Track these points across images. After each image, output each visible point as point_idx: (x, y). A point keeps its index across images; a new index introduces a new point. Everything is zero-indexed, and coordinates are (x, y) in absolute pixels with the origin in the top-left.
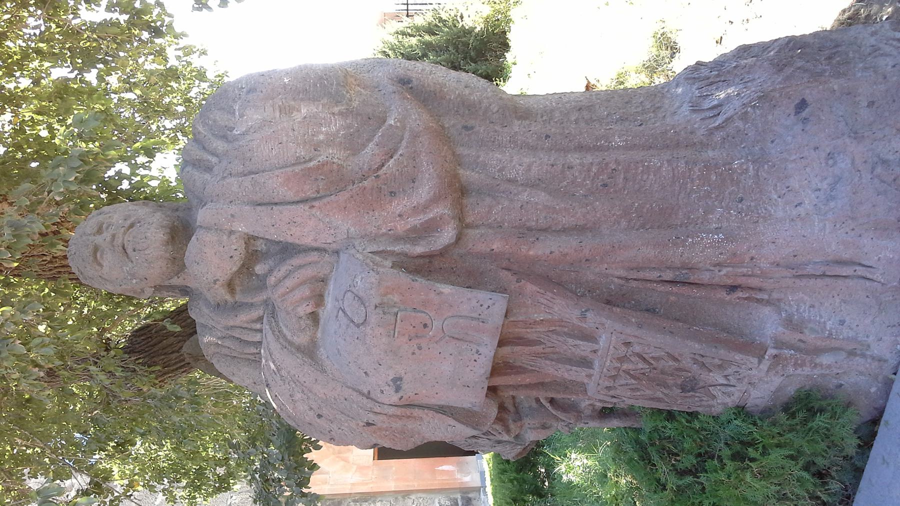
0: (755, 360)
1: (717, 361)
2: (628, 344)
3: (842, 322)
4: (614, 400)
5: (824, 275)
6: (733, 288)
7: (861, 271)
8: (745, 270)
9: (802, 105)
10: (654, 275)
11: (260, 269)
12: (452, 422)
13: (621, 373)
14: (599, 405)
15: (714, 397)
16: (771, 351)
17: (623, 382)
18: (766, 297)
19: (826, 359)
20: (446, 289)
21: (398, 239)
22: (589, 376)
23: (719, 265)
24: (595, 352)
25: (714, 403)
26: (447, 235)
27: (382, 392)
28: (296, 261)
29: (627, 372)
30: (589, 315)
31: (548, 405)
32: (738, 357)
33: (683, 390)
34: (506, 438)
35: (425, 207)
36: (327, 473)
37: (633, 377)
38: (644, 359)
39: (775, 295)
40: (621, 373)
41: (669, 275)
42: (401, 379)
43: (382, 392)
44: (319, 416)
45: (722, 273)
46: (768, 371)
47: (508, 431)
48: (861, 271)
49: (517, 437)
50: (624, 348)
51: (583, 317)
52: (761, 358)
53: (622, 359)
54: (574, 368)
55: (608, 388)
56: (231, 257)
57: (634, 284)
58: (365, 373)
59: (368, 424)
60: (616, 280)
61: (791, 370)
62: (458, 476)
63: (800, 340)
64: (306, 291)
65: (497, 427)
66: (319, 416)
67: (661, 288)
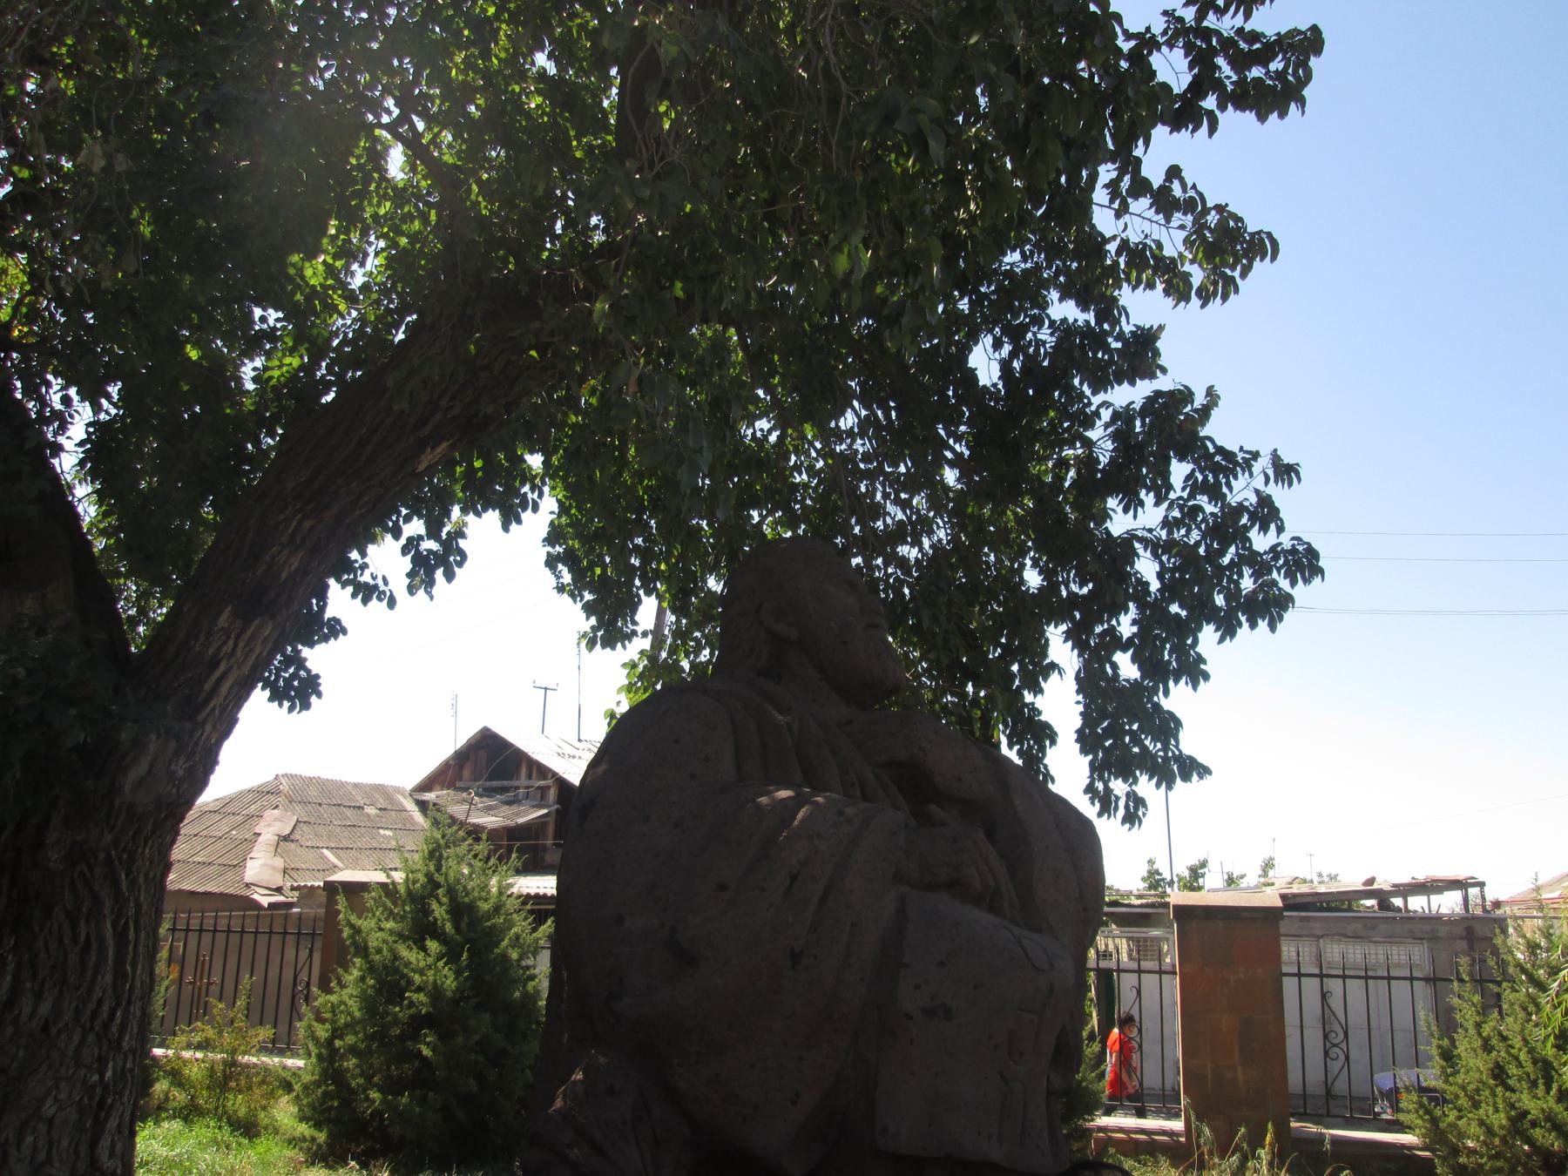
27: (917, 987)
43: (917, 987)
44: (794, 878)
56: (960, 779)
58: (941, 964)
59: (796, 958)
66: (794, 878)
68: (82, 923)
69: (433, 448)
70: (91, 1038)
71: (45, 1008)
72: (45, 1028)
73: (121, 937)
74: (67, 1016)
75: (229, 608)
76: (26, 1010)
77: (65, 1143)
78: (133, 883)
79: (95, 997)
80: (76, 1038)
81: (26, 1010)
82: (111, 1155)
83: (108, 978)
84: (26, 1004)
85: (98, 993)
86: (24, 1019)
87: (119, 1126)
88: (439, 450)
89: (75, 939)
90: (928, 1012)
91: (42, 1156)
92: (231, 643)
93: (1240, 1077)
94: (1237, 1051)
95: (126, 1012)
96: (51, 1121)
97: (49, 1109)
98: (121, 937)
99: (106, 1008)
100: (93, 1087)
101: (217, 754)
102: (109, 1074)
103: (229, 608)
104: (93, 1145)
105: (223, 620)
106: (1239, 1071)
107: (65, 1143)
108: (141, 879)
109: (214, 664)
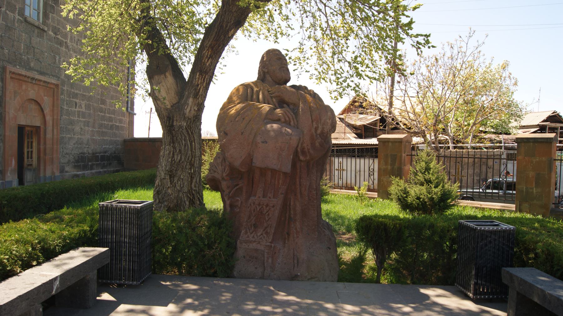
0: (270, 240)
1: (269, 231)
2: (273, 206)
3: (279, 264)
4: (249, 205)
5: (294, 256)
6: (288, 234)
7: (296, 265)
8: (295, 235)
9: (330, 249)
10: (292, 212)
11: (285, 105)
12: (243, 158)
13: (261, 206)
14: (239, 203)
15: (252, 233)
16: (273, 245)
17: (258, 207)
18: (287, 242)
19: (270, 260)
20: (292, 157)
21: (302, 144)
22: (259, 197)
23: (296, 229)
24: (270, 198)
25: (249, 234)
26: (302, 158)
28: (294, 116)
29: (262, 207)
30: (283, 195)
31: (237, 187)
32: (271, 237)
33: (254, 224)
34: (224, 175)
35: (309, 152)
36: (14, 100)
37: (260, 209)
38: (267, 212)
39: (286, 245)
40: (261, 206)
41: (292, 216)
42: (267, 143)
44: (244, 119)
45: (295, 230)
46: (266, 245)
47: (226, 176)
48: (296, 265)
49: (223, 179)
50: (272, 205)
51: (282, 194)
52: (271, 243)
53: (267, 206)
54: (262, 192)
55: (254, 203)
57: (288, 207)
60: (289, 203)
61: (267, 251)
62: (10, 169)
63: (275, 253)
64: (287, 119)
65: (228, 173)
67: (287, 215)
68: (183, 141)
69: (231, 31)
70: (188, 164)
71: (179, 158)
72: (179, 162)
73: (191, 144)
74: (183, 159)
75: (198, 74)
76: (176, 158)
77: (186, 183)
78: (192, 133)
79: (188, 156)
80: (185, 164)
81: (176, 158)
82: (195, 187)
83: (190, 152)
84: (176, 157)
85: (188, 156)
86: (175, 160)
87: (196, 181)
88: (232, 31)
89: (183, 144)
90: (263, 142)
91: (182, 186)
92: (200, 80)
93: (535, 191)
94: (534, 183)
95: (194, 159)
96: (183, 179)
97: (182, 177)
98: (191, 144)
99: (190, 158)
100: (189, 173)
101: (204, 105)
102: (192, 171)
103: (198, 74)
104: (191, 184)
105: (197, 76)
106: (534, 189)
107: (186, 183)
108: (194, 132)
109: (198, 85)
